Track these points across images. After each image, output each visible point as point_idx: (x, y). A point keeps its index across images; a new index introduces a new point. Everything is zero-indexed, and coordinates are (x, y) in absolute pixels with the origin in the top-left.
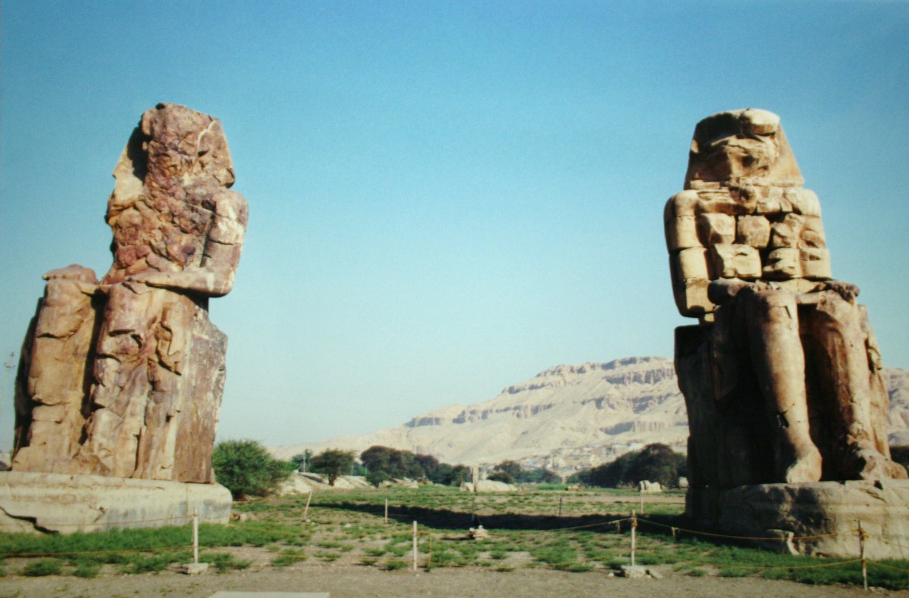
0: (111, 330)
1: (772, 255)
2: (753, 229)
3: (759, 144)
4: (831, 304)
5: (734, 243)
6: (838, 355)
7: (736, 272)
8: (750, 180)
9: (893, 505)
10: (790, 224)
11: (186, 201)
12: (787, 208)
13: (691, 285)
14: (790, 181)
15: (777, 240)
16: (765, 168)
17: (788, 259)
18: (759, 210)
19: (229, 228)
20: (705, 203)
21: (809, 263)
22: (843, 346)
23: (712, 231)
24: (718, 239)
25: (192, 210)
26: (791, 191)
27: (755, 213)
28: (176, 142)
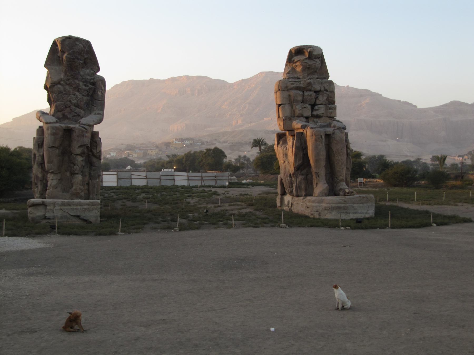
0: (79, 145)
1: (316, 107)
2: (309, 98)
5: (302, 103)
8: (309, 77)
11: (83, 82)
12: (323, 89)
15: (318, 102)
17: (321, 110)
18: (312, 89)
19: (102, 93)
25: (85, 86)
27: (310, 90)
28: (78, 56)
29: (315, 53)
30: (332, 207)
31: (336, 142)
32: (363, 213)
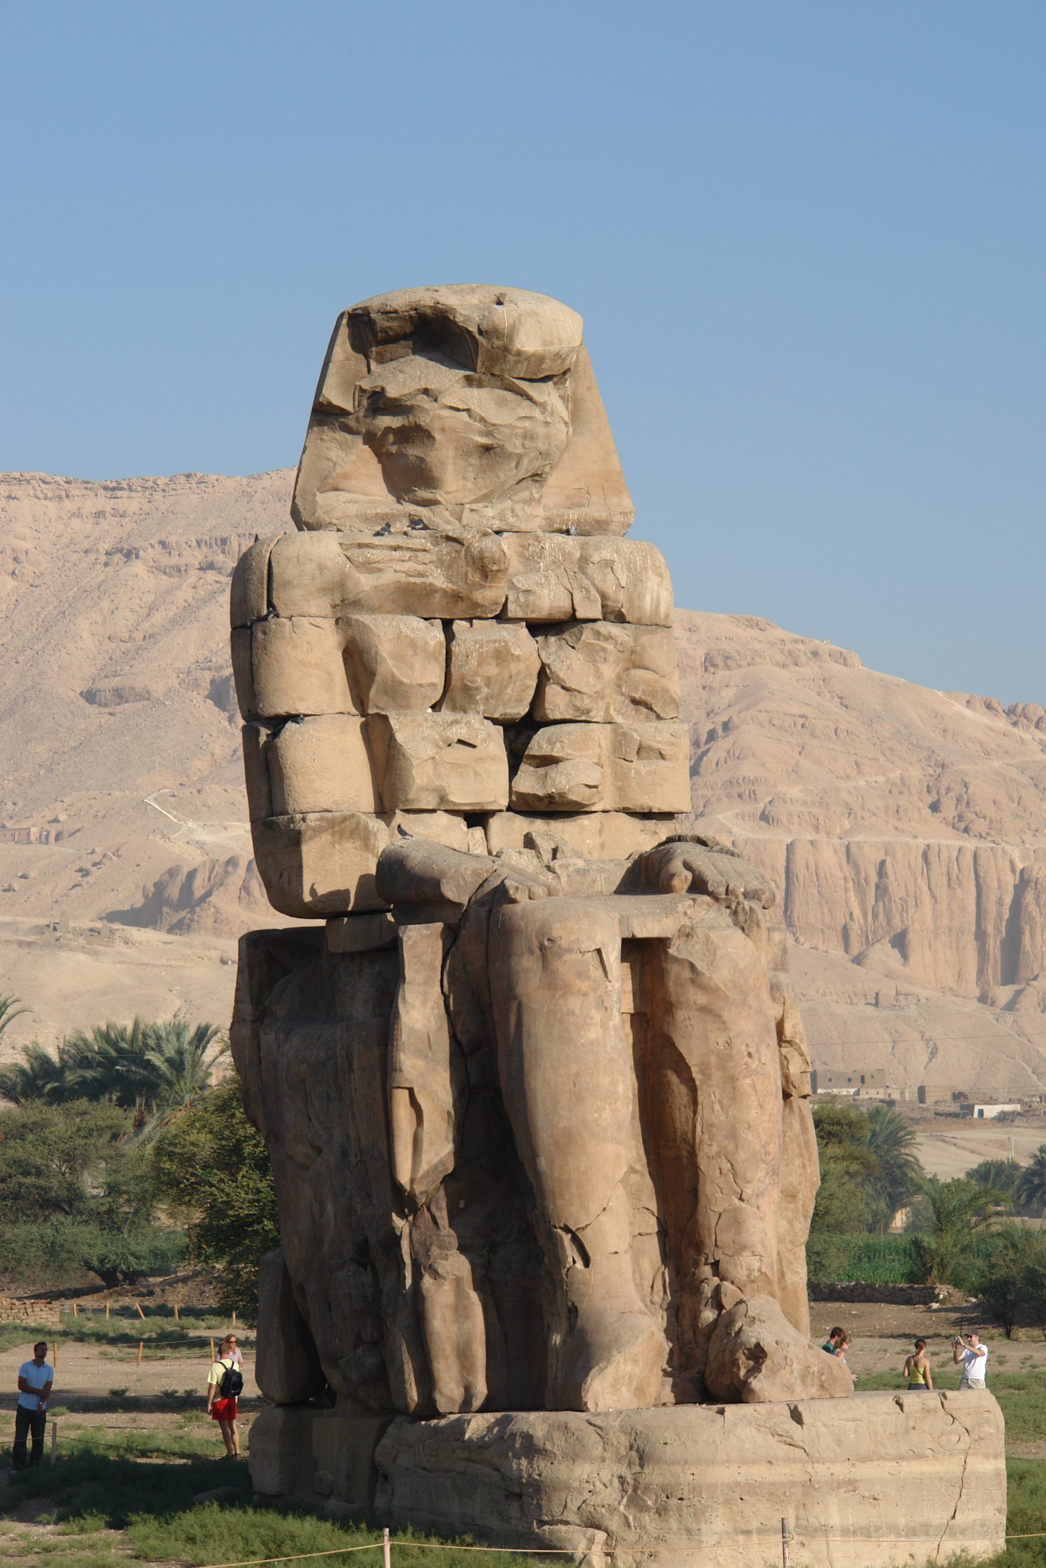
1: (541, 743)
2: (492, 670)
3: (525, 408)
4: (707, 940)
6: (717, 1075)
7: (443, 799)
8: (490, 514)
9: (821, 1460)
10: (593, 654)
13: (318, 831)
14: (596, 511)
16: (537, 477)
18: (513, 611)
20: (365, 583)
21: (639, 767)
22: (726, 1058)
23: (381, 670)
24: (397, 692)
26: (604, 549)
27: (502, 617)
29: (527, 342)
30: (696, 1489)
31: (701, 999)
32: (926, 1530)
